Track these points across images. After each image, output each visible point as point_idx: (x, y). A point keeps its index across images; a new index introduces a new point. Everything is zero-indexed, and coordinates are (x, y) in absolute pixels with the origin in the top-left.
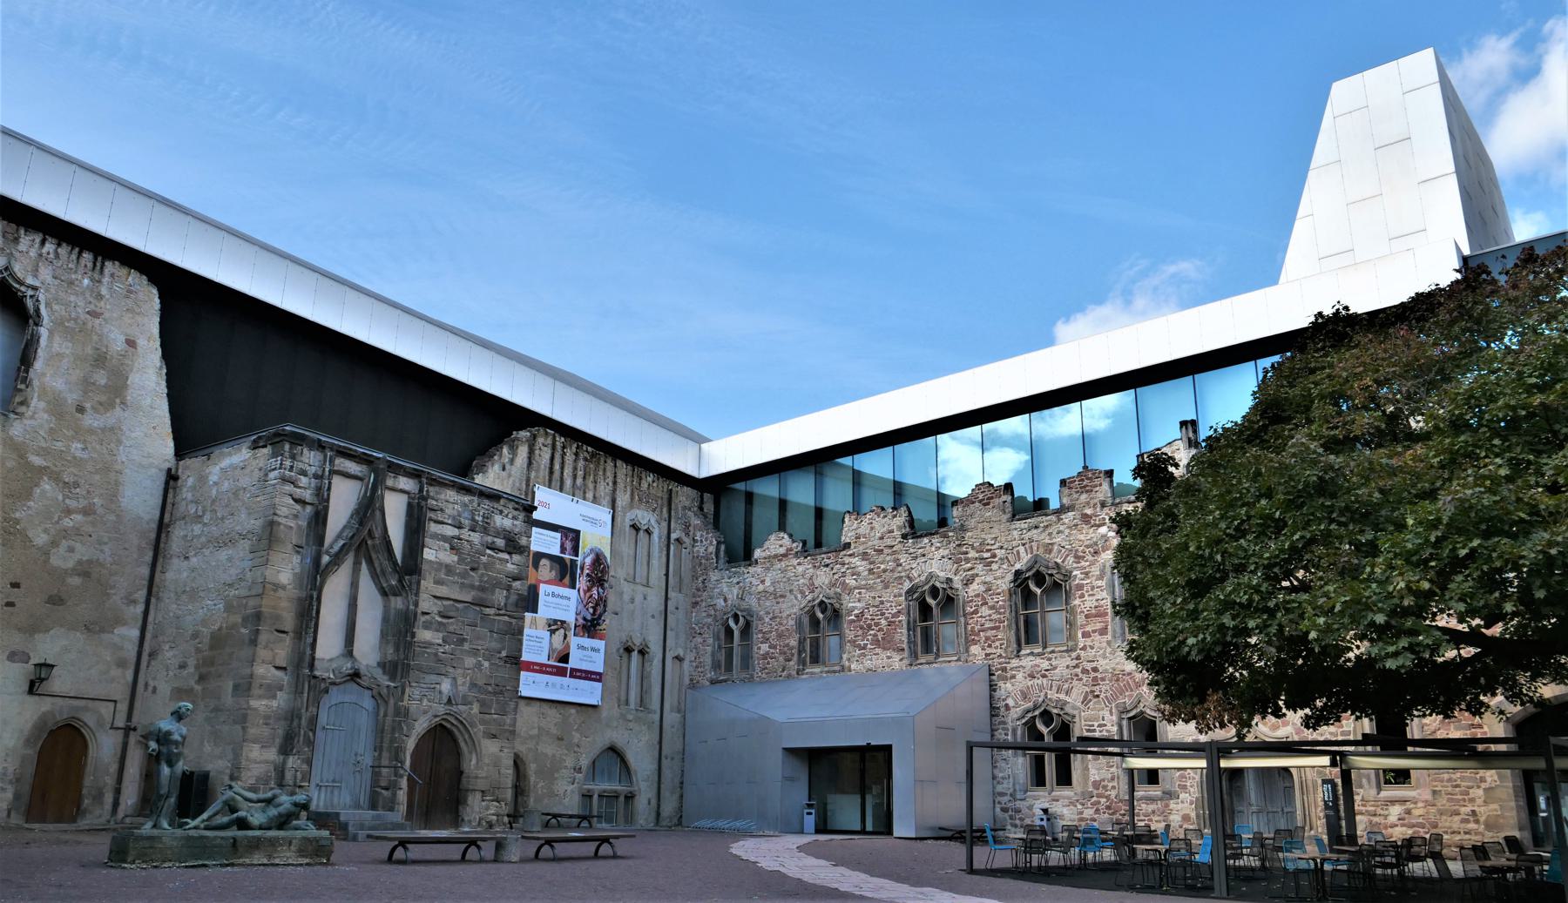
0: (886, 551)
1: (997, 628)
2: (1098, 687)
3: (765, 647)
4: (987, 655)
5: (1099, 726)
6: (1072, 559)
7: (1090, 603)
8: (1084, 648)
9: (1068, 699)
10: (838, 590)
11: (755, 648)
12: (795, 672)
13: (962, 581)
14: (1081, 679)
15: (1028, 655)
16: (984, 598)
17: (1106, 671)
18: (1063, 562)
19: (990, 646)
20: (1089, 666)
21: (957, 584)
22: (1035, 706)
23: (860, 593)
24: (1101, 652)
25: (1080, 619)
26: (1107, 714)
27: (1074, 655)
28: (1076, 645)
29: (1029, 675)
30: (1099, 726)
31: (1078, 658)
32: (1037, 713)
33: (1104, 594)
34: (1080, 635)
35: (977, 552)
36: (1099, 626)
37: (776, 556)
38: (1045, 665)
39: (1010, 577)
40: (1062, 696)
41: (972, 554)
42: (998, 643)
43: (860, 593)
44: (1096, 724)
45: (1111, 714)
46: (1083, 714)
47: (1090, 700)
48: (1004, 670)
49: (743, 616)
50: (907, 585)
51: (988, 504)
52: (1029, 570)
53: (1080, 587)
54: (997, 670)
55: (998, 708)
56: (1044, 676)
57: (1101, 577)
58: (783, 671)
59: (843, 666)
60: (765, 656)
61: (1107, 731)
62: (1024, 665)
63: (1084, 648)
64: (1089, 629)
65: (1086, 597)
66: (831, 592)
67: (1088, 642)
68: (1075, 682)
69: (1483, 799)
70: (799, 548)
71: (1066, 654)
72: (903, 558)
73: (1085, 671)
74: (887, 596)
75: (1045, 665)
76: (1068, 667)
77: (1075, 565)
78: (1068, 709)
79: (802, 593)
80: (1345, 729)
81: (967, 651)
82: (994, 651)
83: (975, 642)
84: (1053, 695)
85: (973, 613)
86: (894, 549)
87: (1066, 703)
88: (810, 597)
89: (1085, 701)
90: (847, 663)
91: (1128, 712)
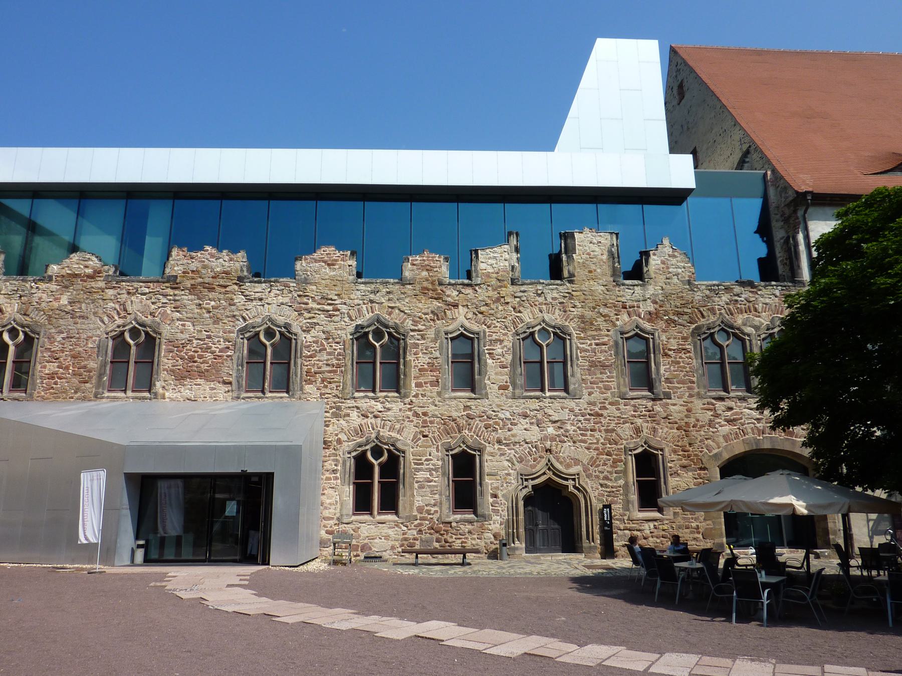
0: (218, 289)
1: (335, 372)
2: (427, 429)
3: (52, 367)
4: (321, 394)
5: (427, 460)
6: (411, 322)
7: (424, 360)
8: (416, 396)
9: (398, 436)
10: (157, 319)
11: (38, 367)
12: (92, 396)
13: (301, 327)
14: (412, 421)
15: (364, 397)
16: (322, 345)
17: (433, 416)
18: (403, 323)
19: (326, 387)
20: (420, 411)
21: (295, 328)
22: (367, 441)
23: (183, 325)
24: (431, 400)
25: (414, 372)
26: (434, 451)
27: (407, 400)
28: (410, 393)
29: (362, 415)
30: (427, 460)
31: (411, 403)
32: (368, 447)
33: (437, 354)
34: (413, 385)
35: (319, 304)
36: (431, 378)
37: (76, 276)
38: (379, 406)
39: (351, 329)
40: (394, 434)
41: (312, 305)
42: (334, 385)
43: (183, 325)
44: (424, 458)
45: (438, 451)
46: (412, 450)
47: (420, 439)
48: (339, 408)
49: (23, 331)
50: (241, 324)
51: (333, 265)
52: (369, 326)
53: (416, 346)
54: (332, 408)
55: (330, 442)
56: (376, 417)
57: (435, 340)
58: (76, 392)
59: (156, 394)
60: (52, 376)
61: (433, 465)
62: (359, 405)
63: (416, 396)
64: (421, 380)
65: (420, 355)
66: (148, 320)
67: (421, 391)
68: (406, 423)
69: (703, 517)
70: (111, 273)
71: (399, 400)
72: (239, 299)
73: (416, 415)
74: (217, 331)
75: (379, 406)
76: (400, 410)
77: (413, 327)
78: (399, 445)
79: (110, 317)
80: (619, 469)
81: (302, 389)
82: (329, 391)
83: (310, 382)
84: (385, 433)
85: (311, 356)
86: (228, 289)
87: (398, 440)
88: (120, 322)
89: (415, 439)
90: (161, 391)
91: (452, 450)
